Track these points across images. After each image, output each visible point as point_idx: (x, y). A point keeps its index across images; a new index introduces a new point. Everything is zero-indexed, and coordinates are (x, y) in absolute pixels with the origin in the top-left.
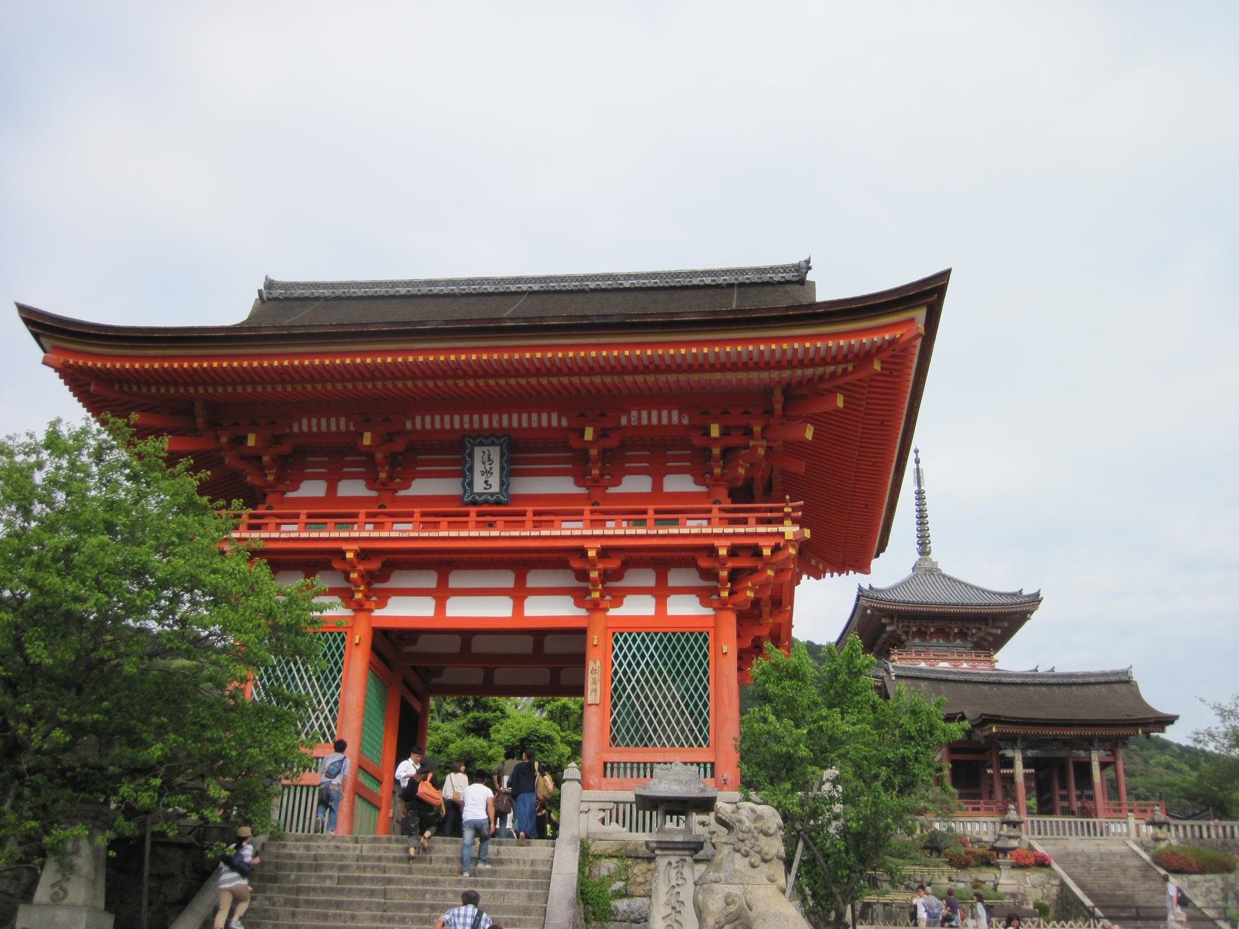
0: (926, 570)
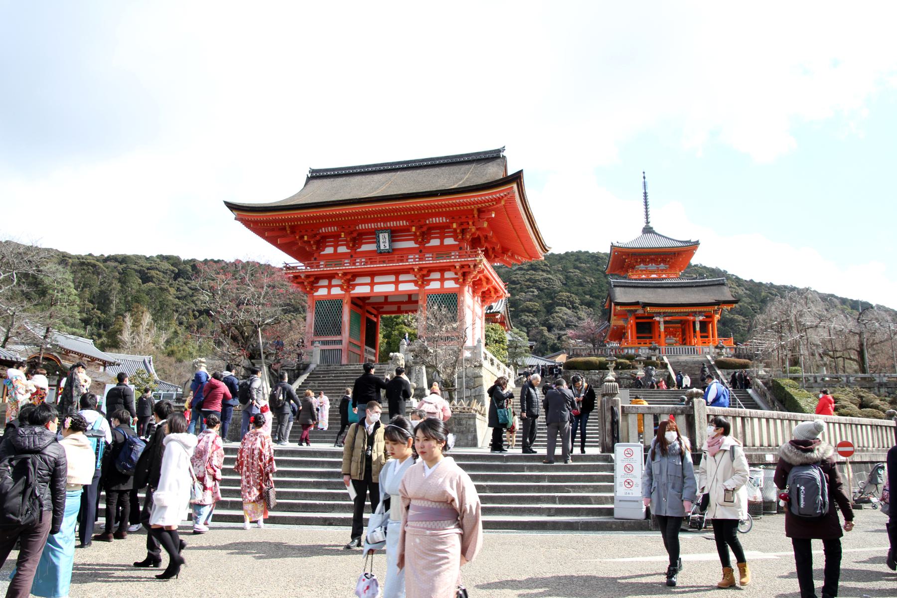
0: (648, 230)
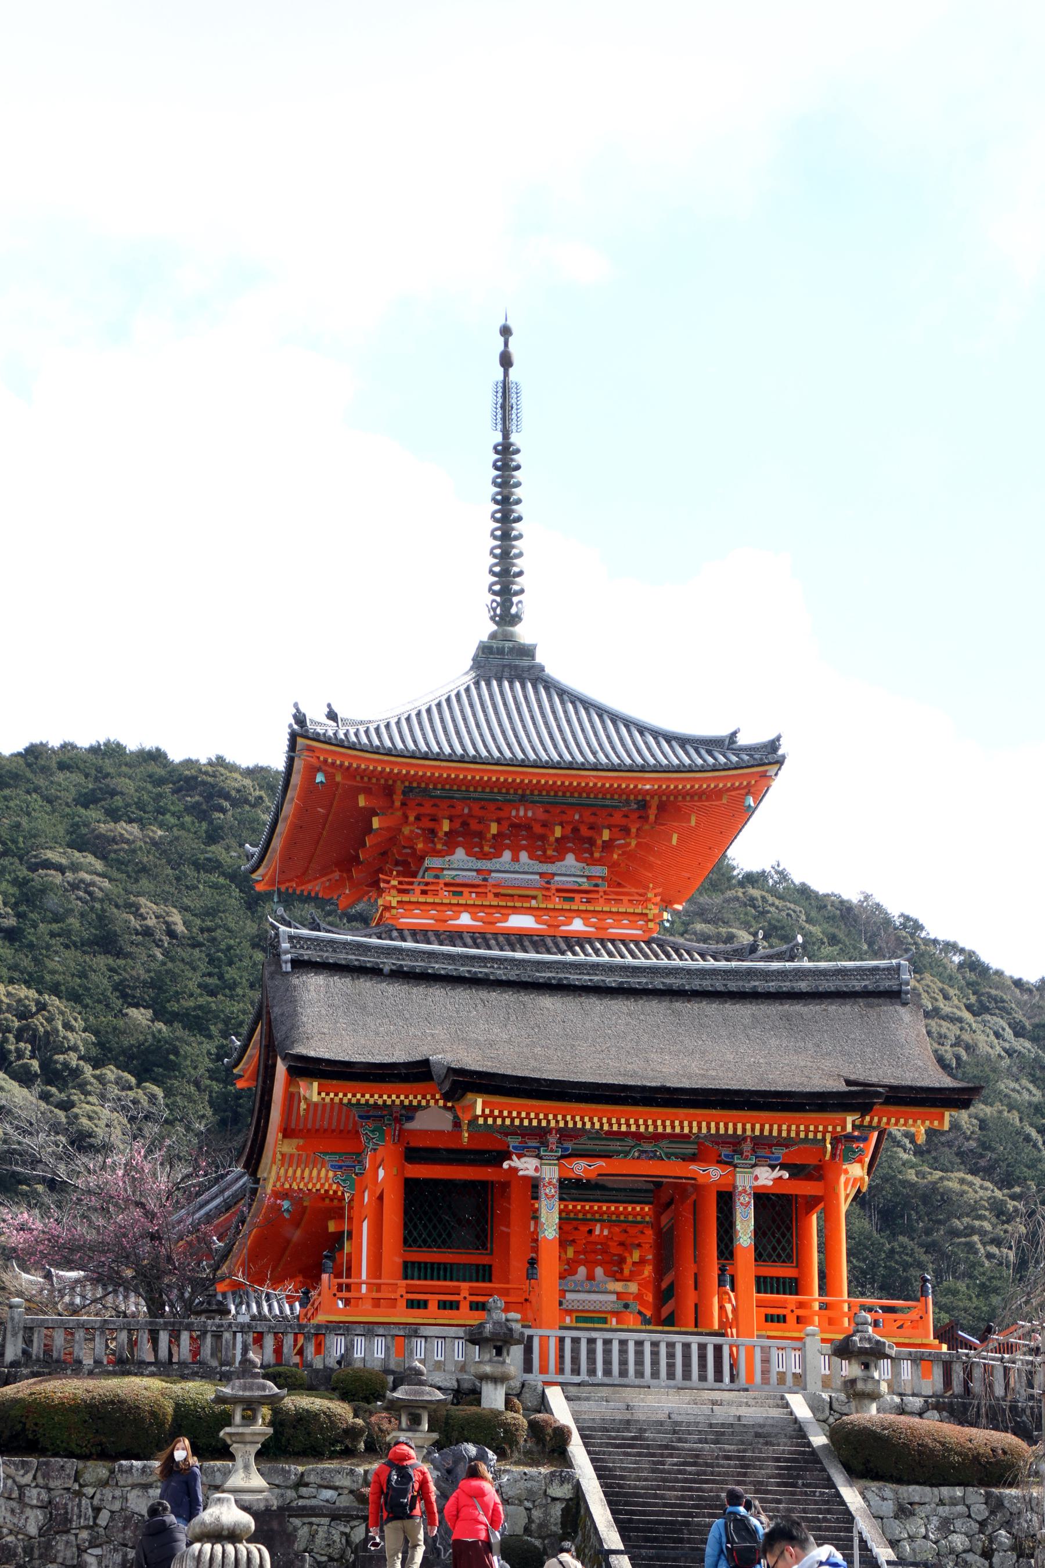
0: (504, 661)
